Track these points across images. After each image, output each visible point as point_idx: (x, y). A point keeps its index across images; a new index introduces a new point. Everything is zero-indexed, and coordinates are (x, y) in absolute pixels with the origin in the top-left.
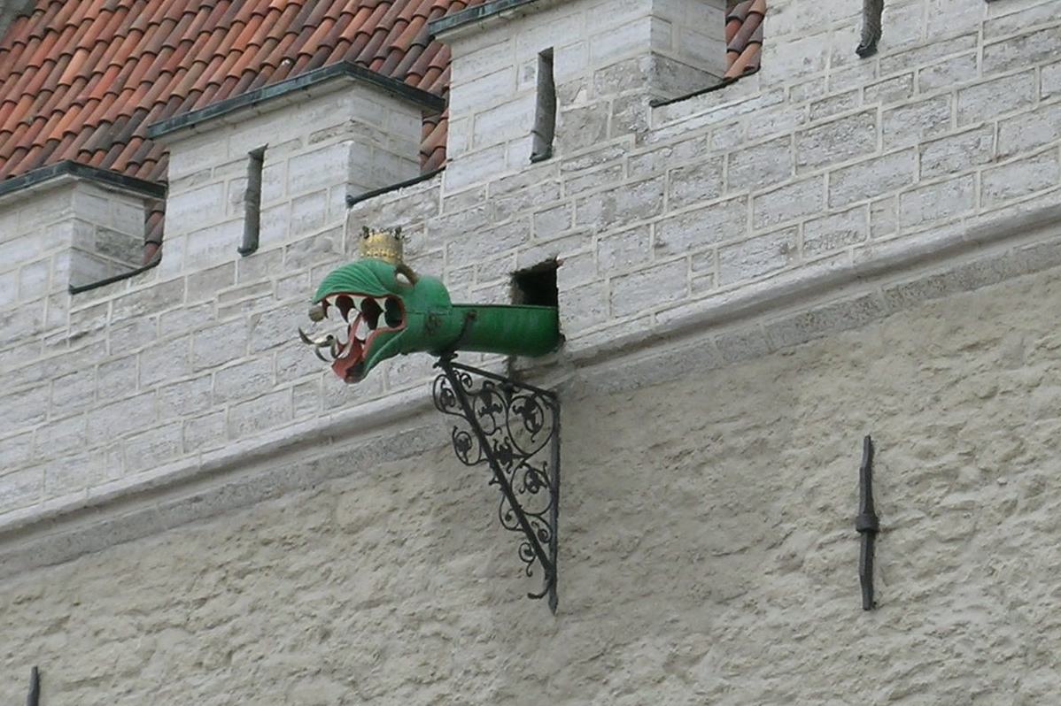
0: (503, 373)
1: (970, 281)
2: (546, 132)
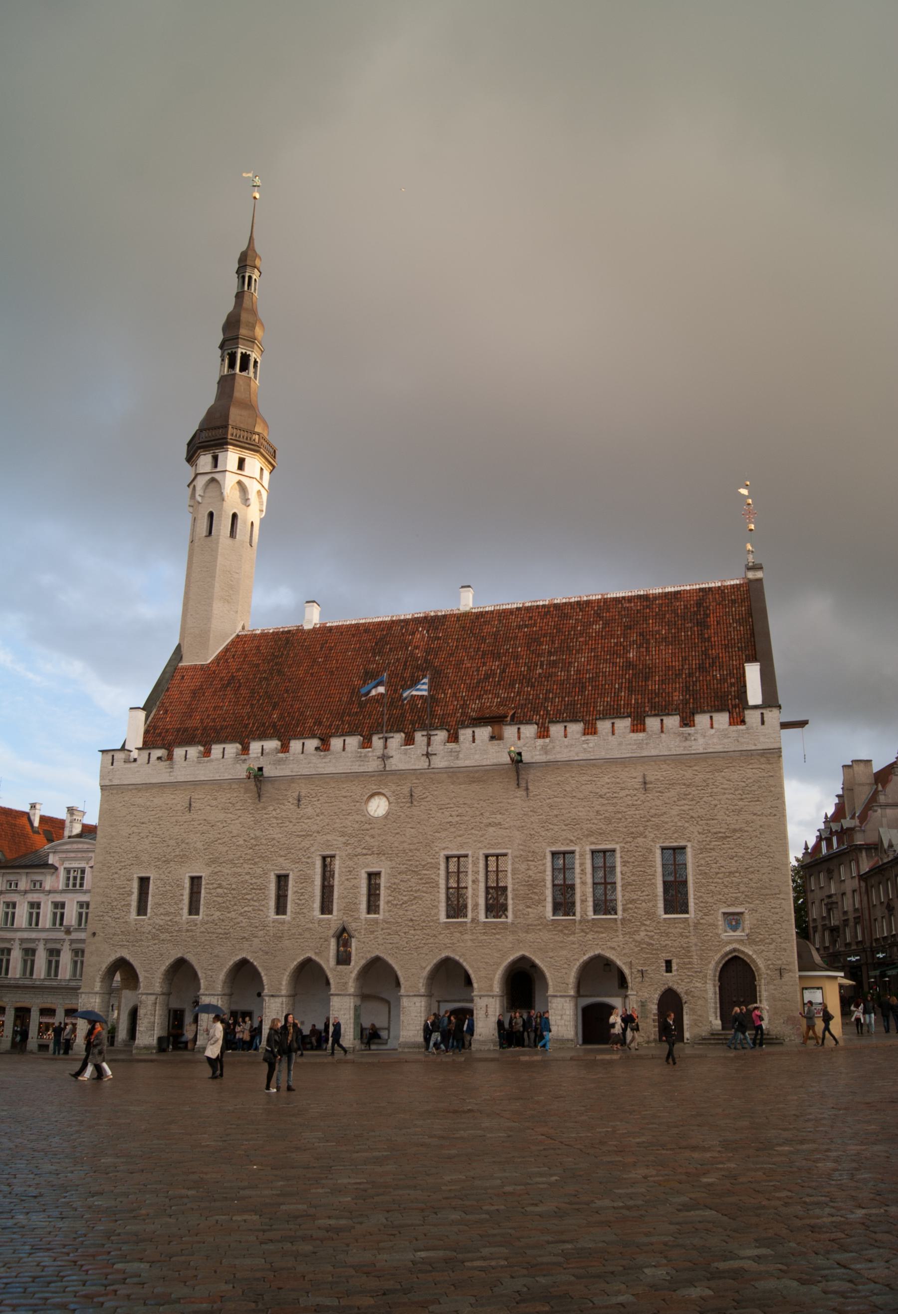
0: (258, 776)
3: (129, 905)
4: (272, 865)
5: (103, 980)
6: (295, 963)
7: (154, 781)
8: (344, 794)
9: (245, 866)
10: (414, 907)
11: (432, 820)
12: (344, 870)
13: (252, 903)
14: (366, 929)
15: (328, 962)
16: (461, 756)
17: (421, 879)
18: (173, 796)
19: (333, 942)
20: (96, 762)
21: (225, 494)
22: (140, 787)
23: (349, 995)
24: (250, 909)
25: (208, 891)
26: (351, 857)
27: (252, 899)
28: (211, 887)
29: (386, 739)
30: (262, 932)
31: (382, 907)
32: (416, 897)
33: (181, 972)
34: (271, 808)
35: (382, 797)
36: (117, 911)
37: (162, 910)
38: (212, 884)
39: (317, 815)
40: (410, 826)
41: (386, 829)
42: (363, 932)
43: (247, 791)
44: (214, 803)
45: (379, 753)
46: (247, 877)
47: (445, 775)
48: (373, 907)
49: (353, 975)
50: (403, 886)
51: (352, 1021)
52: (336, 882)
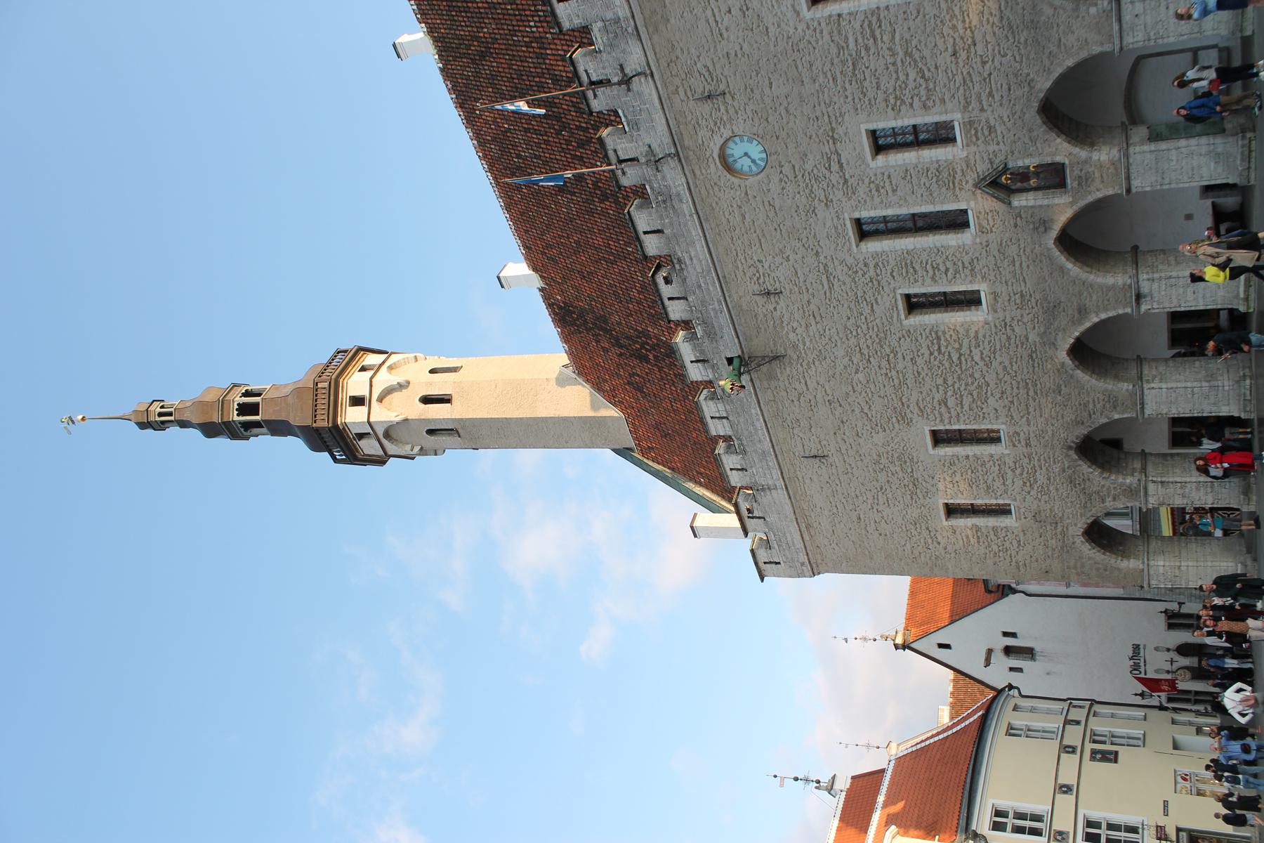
1: (724, 277)
2: (704, 361)
3: (995, 529)
4: (891, 324)
5: (1125, 555)
6: (1069, 265)
7: (788, 509)
8: (739, 218)
9: (900, 366)
10: (926, 53)
11: (746, 46)
12: (877, 201)
13: (965, 350)
14: (986, 142)
15: (1062, 208)
16: (609, 15)
17: (867, 49)
18: (808, 481)
19: (1020, 201)
20: (778, 585)
21: (398, 419)
22: (803, 526)
23: (1127, 156)
24: (976, 352)
25: (954, 420)
26: (850, 191)
27: (959, 350)
28: (946, 416)
29: (621, 162)
30: (1016, 328)
31: (937, 119)
32: (906, 53)
33: (1101, 448)
34: (792, 336)
35: (729, 152)
36: (1007, 544)
37: (998, 484)
38: (941, 415)
39: (788, 259)
40: (767, 91)
41: (783, 135)
42: (992, 147)
43: (771, 377)
44: (804, 423)
45: (649, 172)
46: (919, 361)
47: (656, 38)
48: (941, 136)
49: (1083, 153)
50: (888, 83)
51: (1183, 142)
52: (904, 211)
